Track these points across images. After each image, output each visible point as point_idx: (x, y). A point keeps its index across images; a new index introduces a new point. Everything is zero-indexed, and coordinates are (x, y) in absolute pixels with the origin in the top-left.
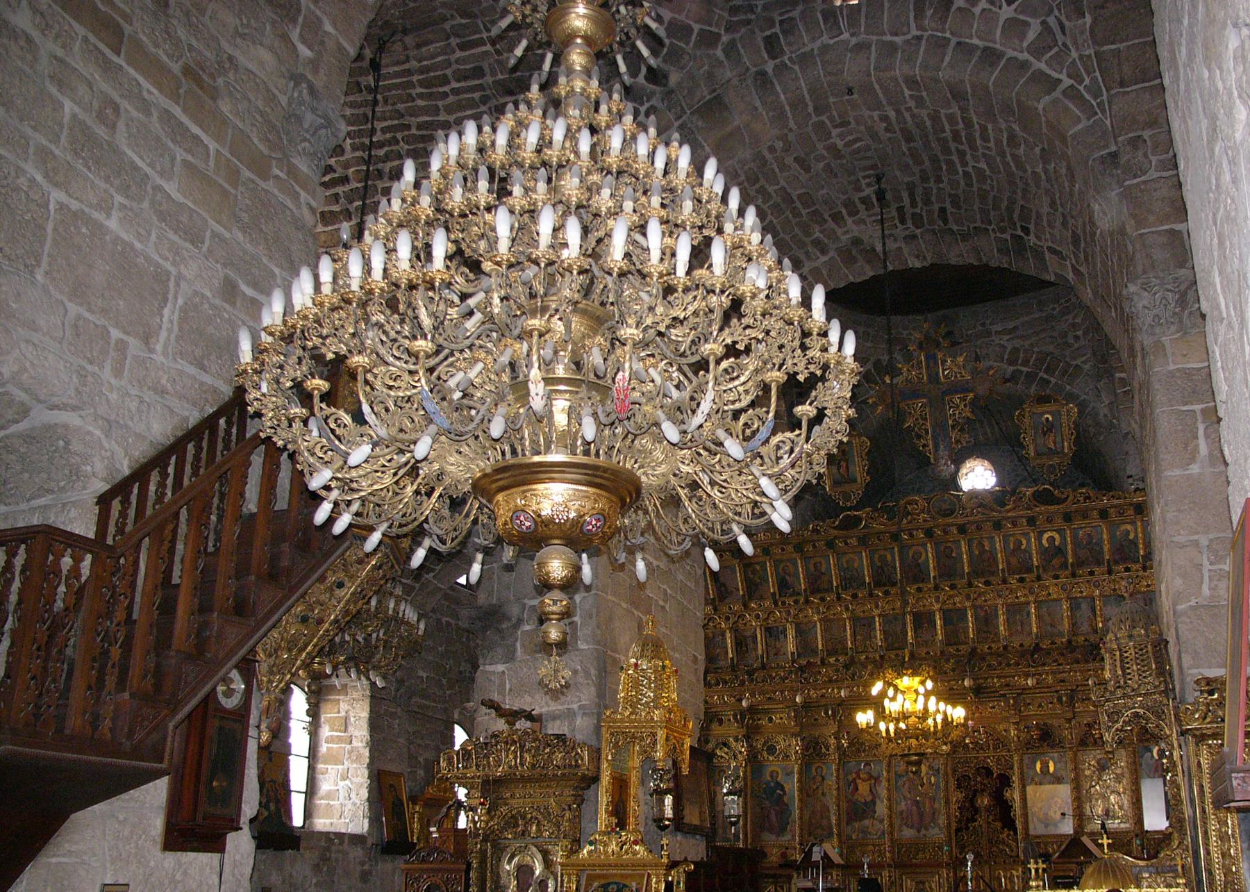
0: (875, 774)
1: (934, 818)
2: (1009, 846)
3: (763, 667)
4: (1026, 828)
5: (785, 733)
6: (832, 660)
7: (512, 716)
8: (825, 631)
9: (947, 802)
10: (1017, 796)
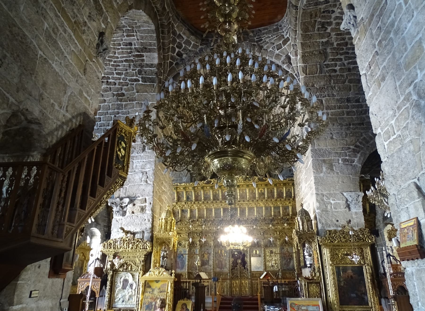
0: (209, 252)
1: (225, 266)
2: (246, 274)
3: (180, 221)
4: (251, 269)
5: (185, 240)
6: (200, 220)
7: (127, 232)
8: (198, 211)
9: (229, 261)
10: (248, 260)
